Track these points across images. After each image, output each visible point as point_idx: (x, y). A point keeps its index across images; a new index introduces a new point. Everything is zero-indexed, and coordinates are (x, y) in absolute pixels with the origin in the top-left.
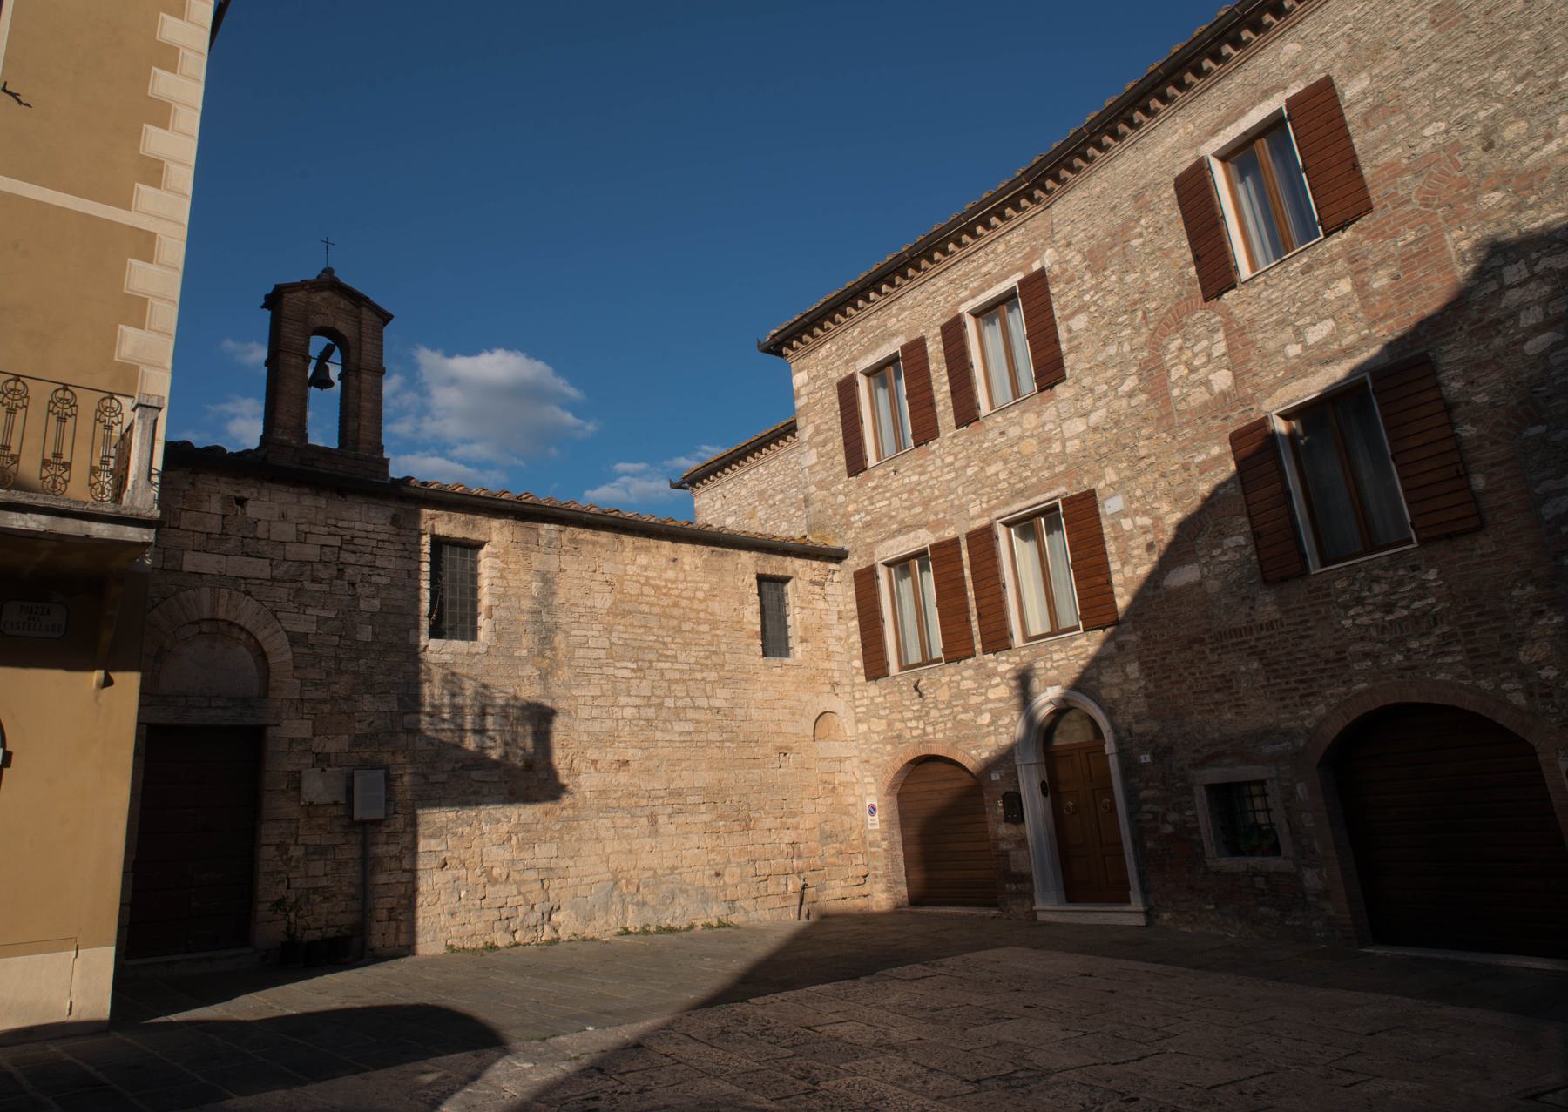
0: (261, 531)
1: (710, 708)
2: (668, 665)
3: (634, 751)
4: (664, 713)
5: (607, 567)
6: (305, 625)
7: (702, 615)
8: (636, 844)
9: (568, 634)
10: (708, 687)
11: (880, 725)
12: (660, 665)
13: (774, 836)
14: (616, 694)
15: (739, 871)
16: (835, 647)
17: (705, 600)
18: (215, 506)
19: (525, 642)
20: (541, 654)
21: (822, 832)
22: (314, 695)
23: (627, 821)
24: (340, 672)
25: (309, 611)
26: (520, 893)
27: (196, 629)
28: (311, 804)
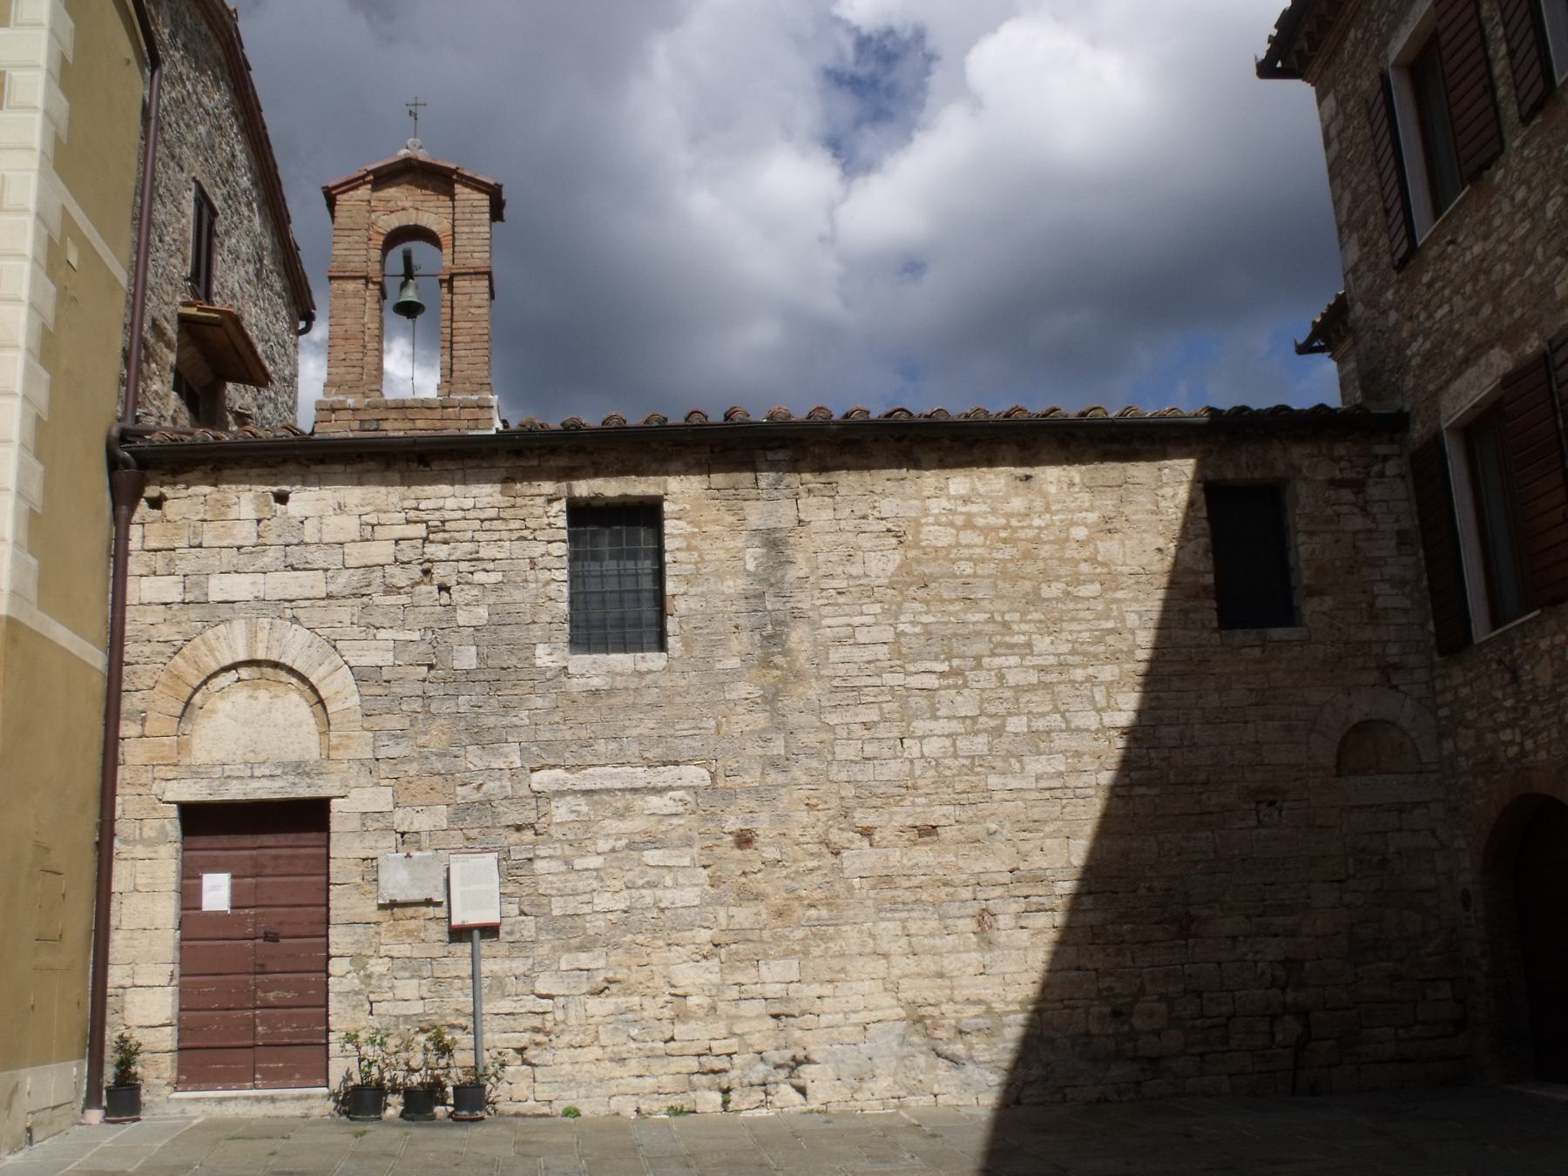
0: (310, 533)
2: (1013, 660)
4: (1004, 744)
5: (887, 506)
6: (375, 654)
8: (949, 964)
9: (815, 626)
10: (1100, 696)
12: (998, 661)
14: (907, 715)
15: (1162, 1007)
16: (1387, 597)
20: (766, 663)
23: (933, 924)
25: (382, 634)
27: (233, 675)
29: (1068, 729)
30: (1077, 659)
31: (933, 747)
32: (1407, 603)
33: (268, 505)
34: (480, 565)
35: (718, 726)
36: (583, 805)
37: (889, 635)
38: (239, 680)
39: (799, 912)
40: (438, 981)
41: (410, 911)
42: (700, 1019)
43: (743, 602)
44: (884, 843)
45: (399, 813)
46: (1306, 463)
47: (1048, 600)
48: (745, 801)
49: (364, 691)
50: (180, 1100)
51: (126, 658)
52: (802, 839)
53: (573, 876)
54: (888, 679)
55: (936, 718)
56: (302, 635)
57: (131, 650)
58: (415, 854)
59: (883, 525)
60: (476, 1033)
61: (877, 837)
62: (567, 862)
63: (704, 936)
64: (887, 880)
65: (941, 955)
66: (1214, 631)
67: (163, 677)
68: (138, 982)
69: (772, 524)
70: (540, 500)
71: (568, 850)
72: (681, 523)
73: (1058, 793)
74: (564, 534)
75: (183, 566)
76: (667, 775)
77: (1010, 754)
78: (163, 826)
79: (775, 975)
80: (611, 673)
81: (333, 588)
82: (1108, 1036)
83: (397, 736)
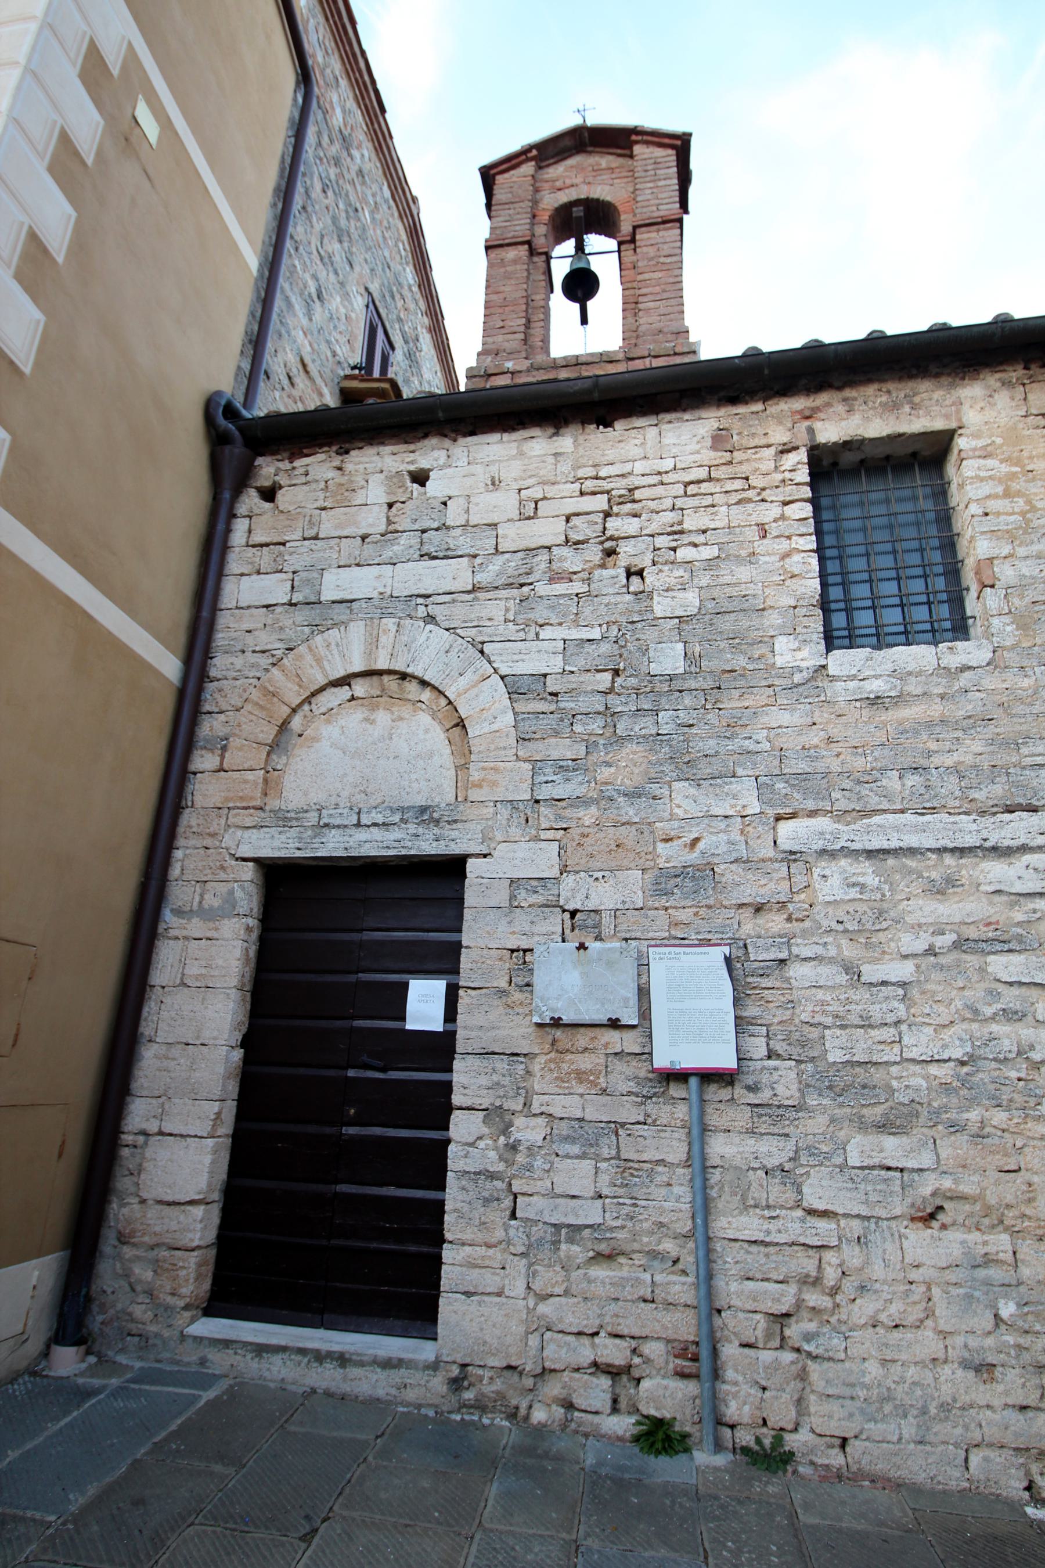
0: (454, 515)
18: (376, 493)
22: (558, 792)
24: (621, 740)
25: (546, 633)
27: (344, 692)
28: (557, 1023)
34: (686, 539)
36: (866, 872)
38: (353, 698)
40: (626, 1166)
41: (582, 1039)
45: (569, 880)
49: (520, 707)
50: (199, 1340)
51: (213, 673)
53: (860, 995)
56: (438, 637)
57: (219, 665)
58: (594, 946)
67: (255, 695)
72: (990, 463)
75: (293, 562)
76: (1018, 828)
78: (231, 892)
81: (482, 578)
83: (566, 768)
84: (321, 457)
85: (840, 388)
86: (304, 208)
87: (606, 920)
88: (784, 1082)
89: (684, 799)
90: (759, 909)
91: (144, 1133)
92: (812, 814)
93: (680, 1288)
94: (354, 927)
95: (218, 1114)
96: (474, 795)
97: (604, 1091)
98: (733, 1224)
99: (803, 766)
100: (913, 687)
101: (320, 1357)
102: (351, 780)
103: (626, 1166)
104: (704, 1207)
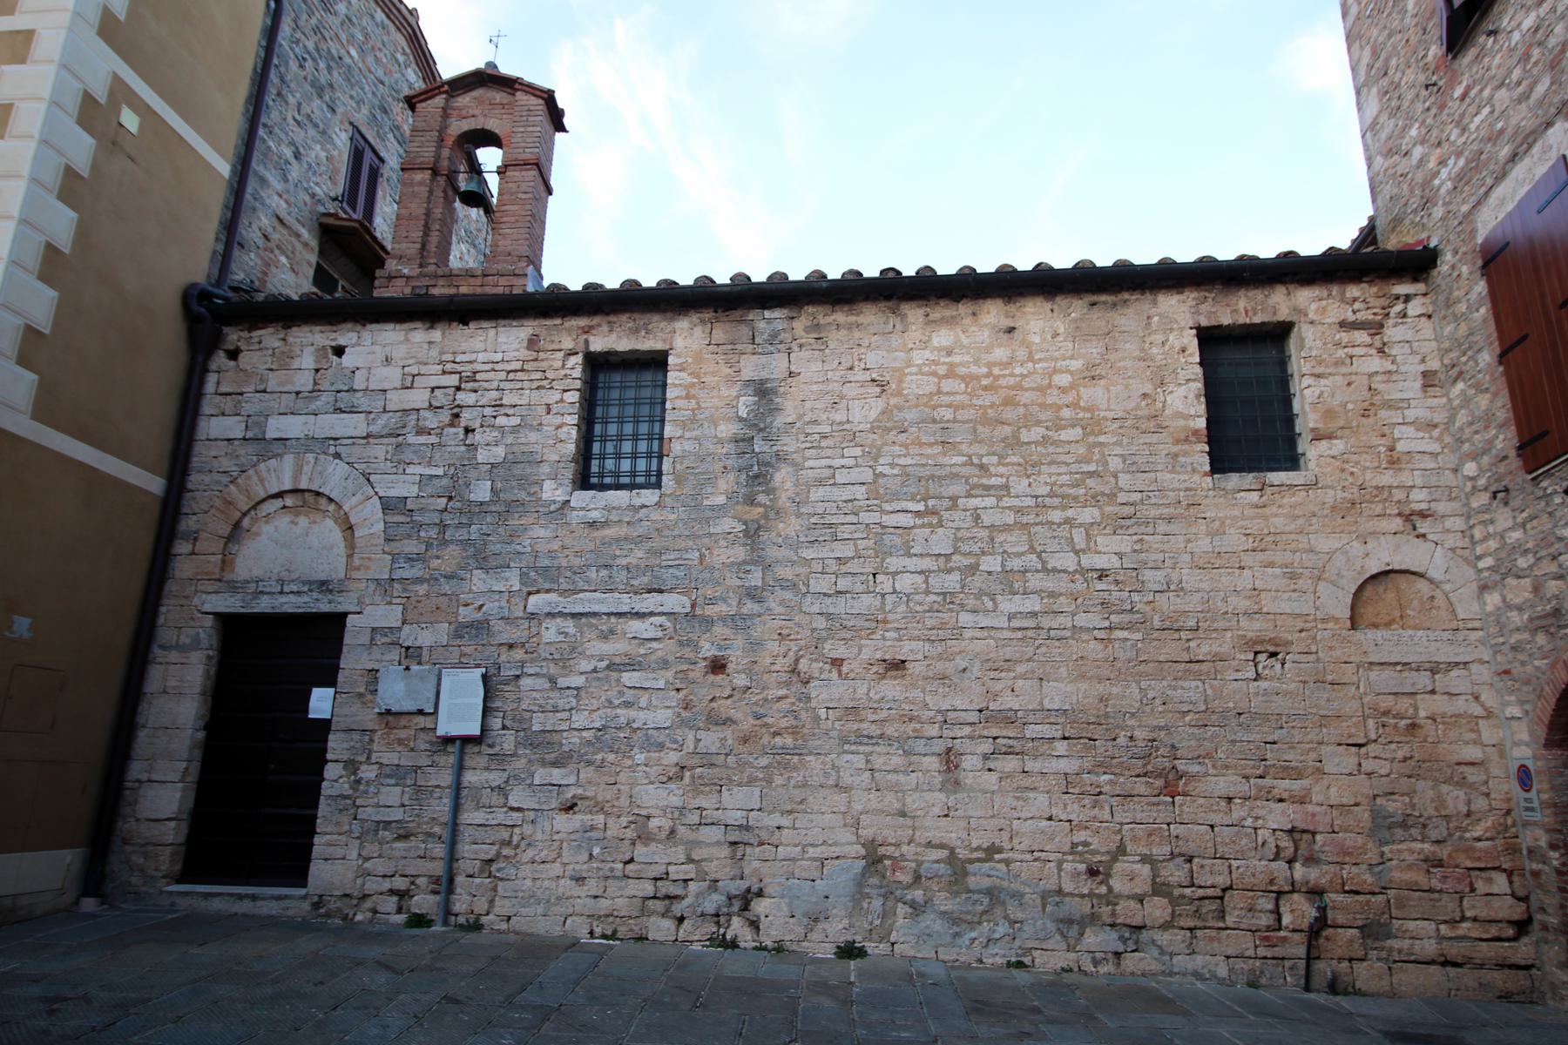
0: (359, 383)
1: (1082, 571)
2: (991, 501)
3: (914, 645)
4: (977, 582)
5: (872, 358)
6: (403, 487)
7: (1066, 413)
8: (913, 802)
10: (1079, 537)
11: (1519, 591)
13: (1238, 812)
14: (882, 553)
15: (1146, 870)
16: (1409, 440)
17: (1072, 386)
18: (307, 361)
19: (722, 484)
20: (751, 501)
21: (1376, 814)
22: (406, 574)
23: (897, 760)
26: (690, 860)
27: (278, 503)
28: (388, 712)
29: (1045, 570)
30: (1056, 501)
31: (905, 583)
32: (1436, 448)
33: (326, 357)
34: (503, 411)
35: (702, 556)
36: (569, 626)
37: (868, 476)
38: (284, 507)
39: (766, 739)
40: (419, 789)
41: (403, 721)
42: (659, 841)
43: (732, 445)
44: (852, 675)
45: (407, 628)
46: (1313, 306)
47: (1028, 443)
48: (719, 630)
49: (388, 519)
50: (171, 893)
51: (190, 486)
52: (774, 668)
53: (556, 694)
54: (865, 517)
55: (910, 555)
56: (340, 468)
57: (194, 480)
58: (415, 668)
59: (867, 376)
60: (453, 844)
61: (845, 669)
62: (553, 680)
63: (672, 757)
64: (853, 711)
65: (904, 792)
66: (1206, 474)
67: (218, 503)
68: (154, 777)
69: (764, 375)
70: (560, 355)
71: (553, 670)
72: (683, 374)
73: (1030, 633)
74: (578, 384)
75: (248, 408)
76: (650, 602)
77: (980, 594)
78: (198, 634)
79: (737, 802)
80: (608, 509)
81: (374, 429)
82: (1083, 896)
84: (271, 330)
85: (608, 314)
86: (279, 94)
87: (425, 652)
88: (508, 742)
89: (479, 581)
90: (511, 646)
91: (139, 781)
92: (548, 591)
93: (439, 850)
94: (281, 654)
95: (186, 769)
96: (355, 575)
97: (412, 750)
98: (470, 816)
99: (546, 562)
100: (614, 518)
101: (241, 897)
102: (282, 559)
103: (419, 789)
104: (456, 808)
